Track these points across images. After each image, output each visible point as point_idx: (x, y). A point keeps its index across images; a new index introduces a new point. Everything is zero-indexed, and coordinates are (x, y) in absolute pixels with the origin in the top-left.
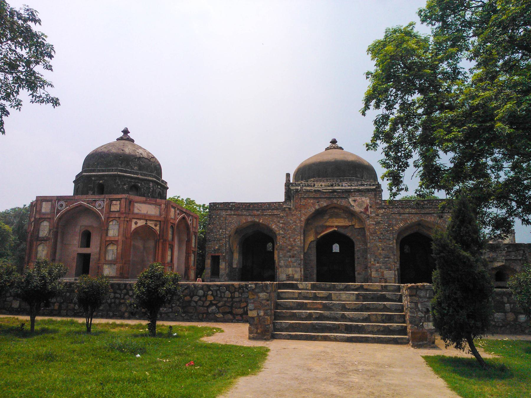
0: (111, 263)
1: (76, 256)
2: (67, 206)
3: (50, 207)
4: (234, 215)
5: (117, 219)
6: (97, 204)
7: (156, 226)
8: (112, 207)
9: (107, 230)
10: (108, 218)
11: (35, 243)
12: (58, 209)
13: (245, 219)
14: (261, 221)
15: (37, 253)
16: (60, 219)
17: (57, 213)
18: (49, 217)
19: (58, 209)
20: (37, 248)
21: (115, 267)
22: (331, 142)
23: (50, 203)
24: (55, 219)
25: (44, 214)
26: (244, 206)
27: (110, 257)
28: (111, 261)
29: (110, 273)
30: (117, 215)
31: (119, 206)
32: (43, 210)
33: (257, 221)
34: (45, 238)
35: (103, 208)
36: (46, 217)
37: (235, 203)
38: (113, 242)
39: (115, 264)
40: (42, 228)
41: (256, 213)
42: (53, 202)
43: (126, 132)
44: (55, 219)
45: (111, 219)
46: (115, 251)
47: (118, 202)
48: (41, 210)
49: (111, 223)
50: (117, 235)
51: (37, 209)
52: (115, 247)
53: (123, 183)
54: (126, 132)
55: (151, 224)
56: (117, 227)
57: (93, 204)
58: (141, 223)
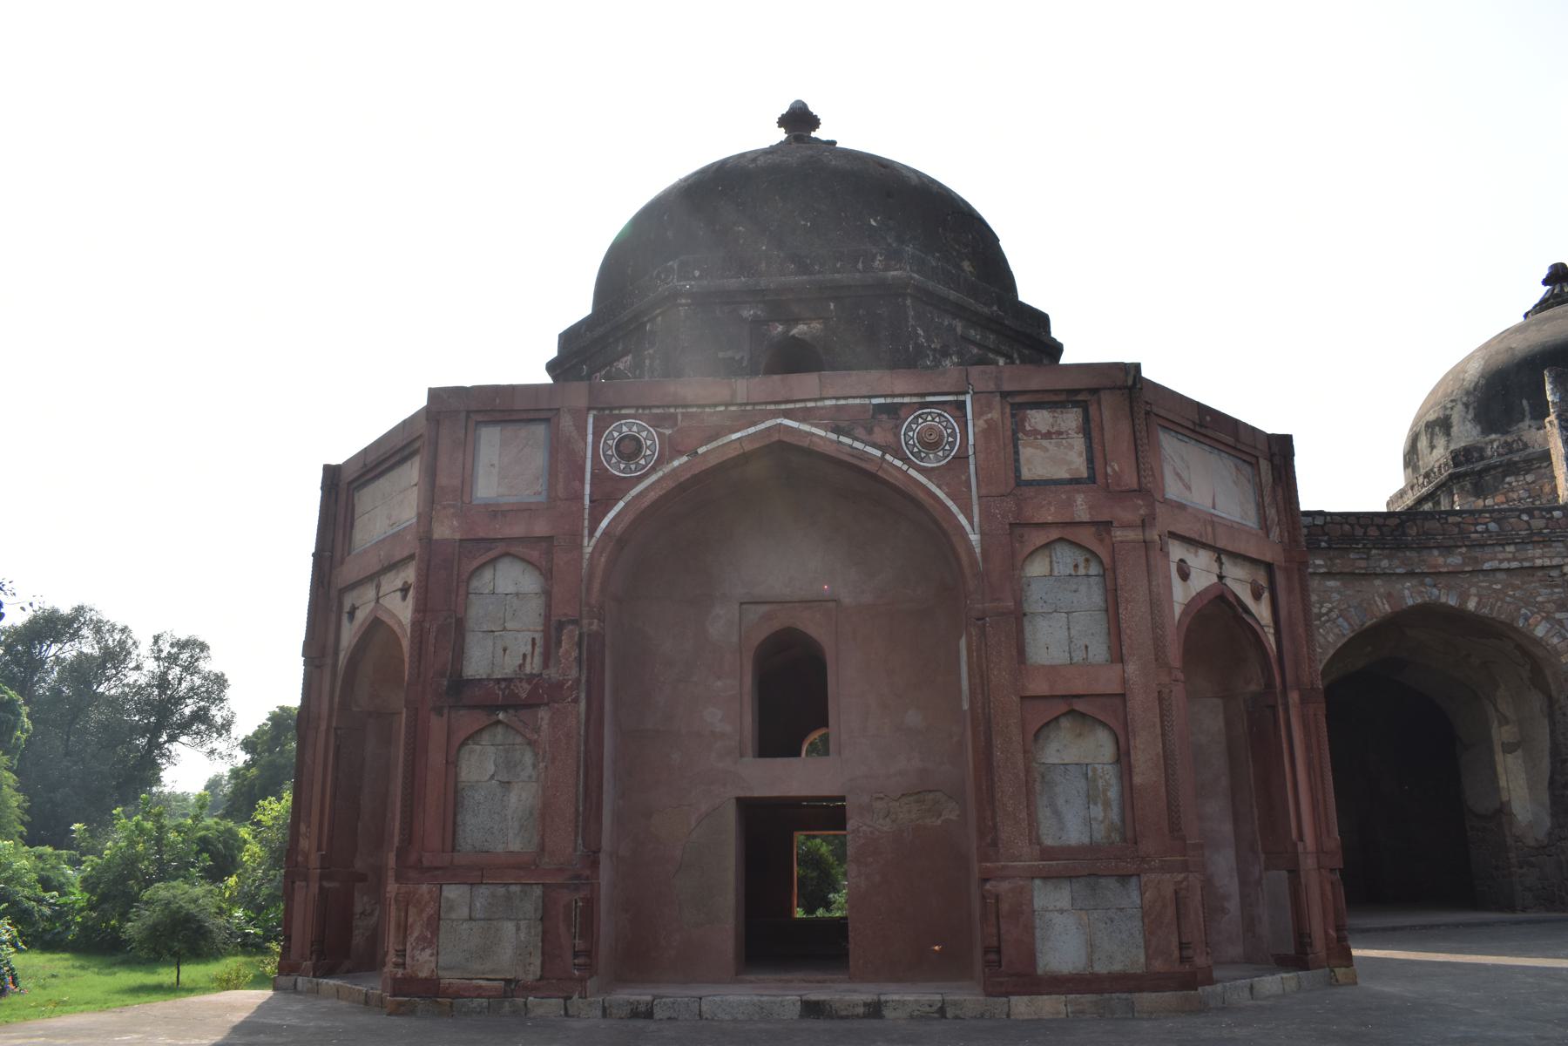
0: (1079, 868)
1: (730, 819)
2: (671, 449)
3: (538, 459)
4: (1329, 575)
5: (1086, 536)
6: (911, 429)
7: (1257, 596)
8: (1026, 452)
9: (1018, 616)
10: (1019, 526)
11: (437, 725)
12: (600, 476)
13: (1389, 596)
14: (1471, 605)
15: (454, 800)
16: (618, 541)
17: (601, 504)
18: (541, 528)
19: (600, 476)
20: (452, 763)
21: (1132, 898)
22: (1545, 282)
23: (540, 430)
24: (588, 547)
25: (495, 512)
26: (1373, 532)
27: (1073, 820)
28: (1090, 851)
29: (1091, 946)
30: (1081, 508)
31: (1079, 443)
32: (487, 488)
33: (1453, 602)
34: (523, 690)
35: (962, 458)
36: (518, 530)
37: (1321, 513)
38: (1075, 709)
39: (1123, 878)
40: (478, 612)
41: (1438, 560)
42: (566, 422)
43: (799, 120)
44: (588, 547)
45: (1040, 538)
46: (1108, 775)
47: (1070, 420)
48: (467, 481)
49: (1037, 568)
50: (1099, 651)
51: (443, 480)
52: (1097, 748)
53: (936, 345)
54: (799, 120)
55: (1239, 581)
56: (1090, 596)
57: (879, 435)
58: (1203, 572)
